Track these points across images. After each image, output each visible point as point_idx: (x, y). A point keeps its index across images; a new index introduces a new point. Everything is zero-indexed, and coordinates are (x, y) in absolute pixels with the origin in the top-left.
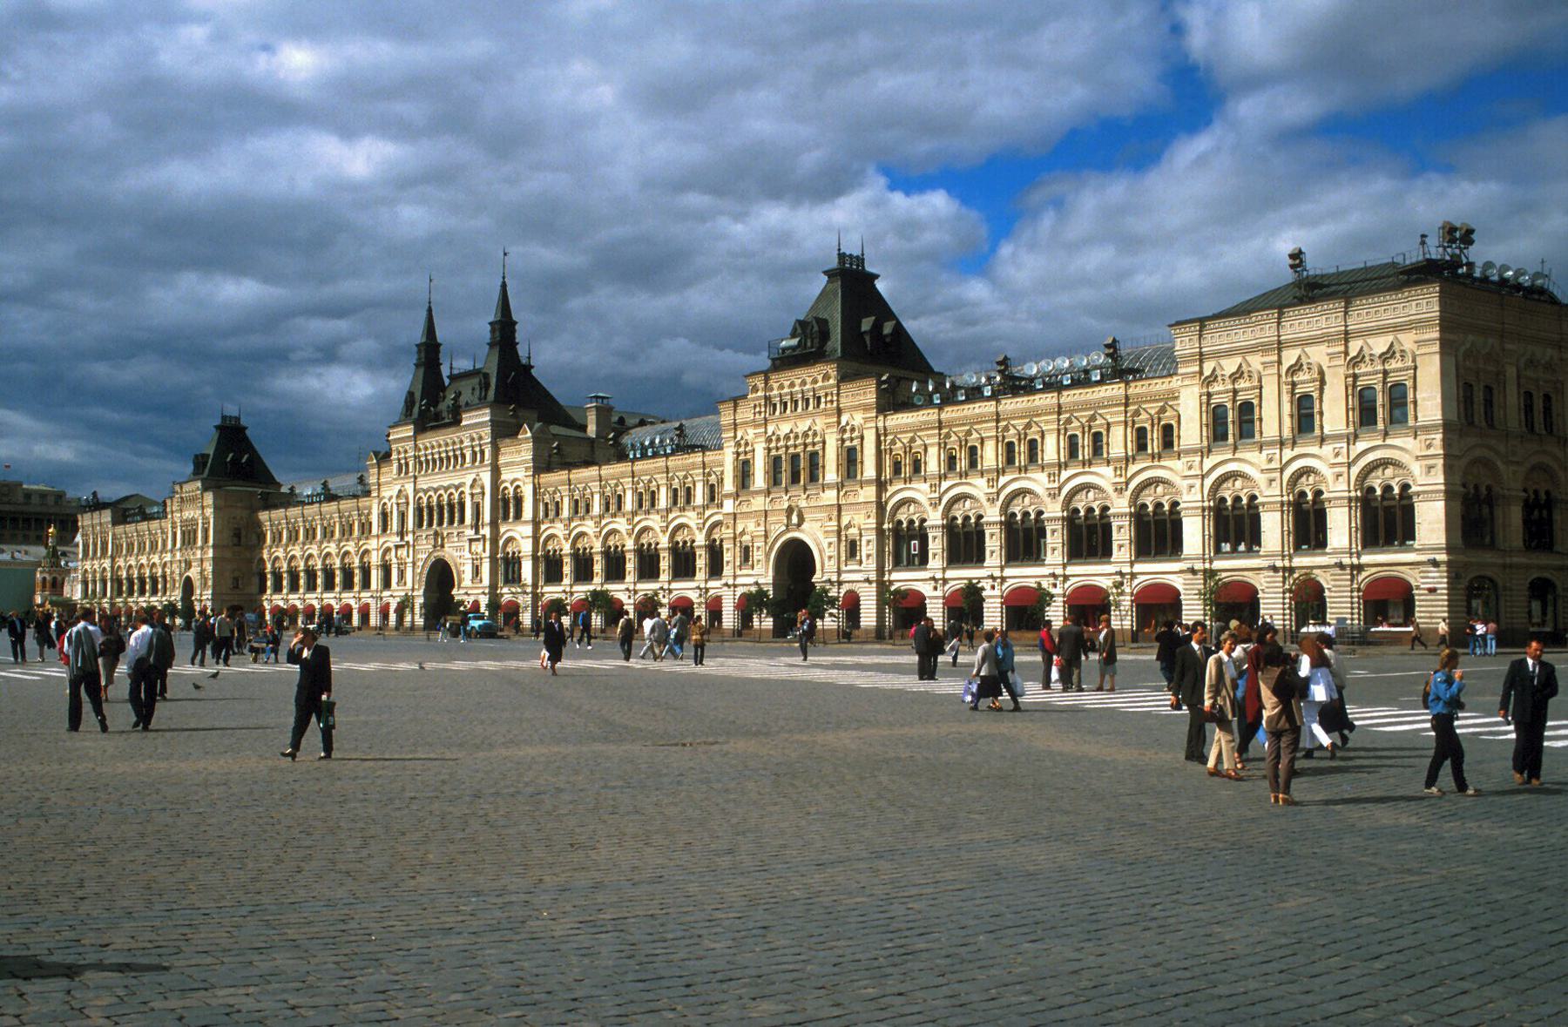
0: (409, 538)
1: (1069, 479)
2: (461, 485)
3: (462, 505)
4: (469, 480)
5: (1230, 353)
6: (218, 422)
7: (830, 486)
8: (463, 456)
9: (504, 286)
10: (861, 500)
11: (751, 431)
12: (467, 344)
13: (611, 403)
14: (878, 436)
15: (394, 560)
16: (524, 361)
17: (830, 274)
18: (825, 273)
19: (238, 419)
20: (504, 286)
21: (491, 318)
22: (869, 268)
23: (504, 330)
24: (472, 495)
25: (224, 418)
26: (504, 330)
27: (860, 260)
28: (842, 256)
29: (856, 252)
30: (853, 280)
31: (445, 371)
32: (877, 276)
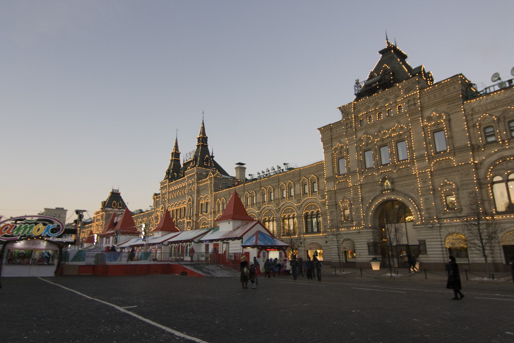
13: (245, 166)
18: (381, 52)
19: (118, 191)
23: (203, 140)
25: (113, 190)
26: (203, 140)
31: (182, 163)
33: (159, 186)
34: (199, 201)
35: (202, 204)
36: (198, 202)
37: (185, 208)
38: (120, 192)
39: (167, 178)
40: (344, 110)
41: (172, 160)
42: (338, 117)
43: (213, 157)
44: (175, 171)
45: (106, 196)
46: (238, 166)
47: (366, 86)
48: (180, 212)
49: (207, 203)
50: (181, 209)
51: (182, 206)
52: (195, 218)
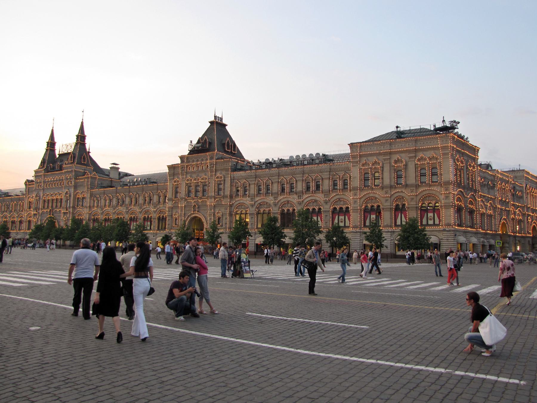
1: (305, 199)
5: (371, 155)
7: (211, 197)
9: (82, 123)
12: (65, 143)
14: (231, 180)
16: (88, 150)
17: (211, 123)
18: (210, 122)
20: (82, 123)
22: (224, 122)
23: (81, 138)
26: (81, 138)
28: (215, 117)
29: (220, 116)
30: (218, 126)
33: (33, 174)
34: (76, 195)
35: (78, 198)
36: (75, 196)
37: (61, 199)
39: (41, 168)
40: (182, 158)
41: (47, 150)
42: (178, 161)
43: (89, 152)
44: (52, 161)
46: (113, 165)
47: (194, 147)
48: (57, 202)
49: (83, 198)
50: (57, 199)
51: (59, 197)
52: (71, 210)
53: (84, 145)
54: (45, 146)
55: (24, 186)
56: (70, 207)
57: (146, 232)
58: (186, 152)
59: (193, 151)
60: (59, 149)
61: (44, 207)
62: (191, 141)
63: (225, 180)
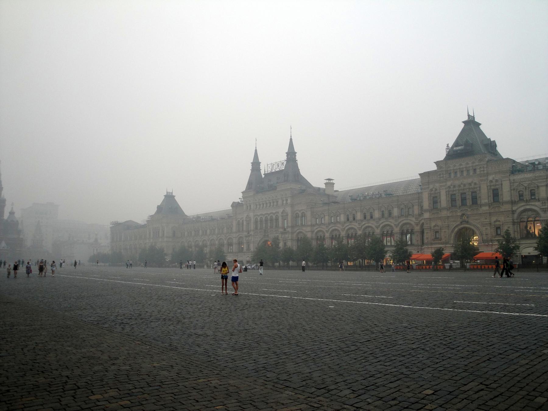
0: (252, 233)
2: (278, 212)
3: (277, 219)
4: (281, 210)
6: (165, 194)
7: (485, 205)
8: (277, 202)
10: (501, 210)
11: (437, 185)
13: (333, 181)
15: (245, 241)
18: (463, 122)
20: (291, 140)
21: (287, 151)
23: (291, 155)
24: (282, 216)
26: (291, 155)
27: (474, 117)
28: (469, 115)
31: (262, 172)
32: (480, 124)
33: (241, 195)
38: (174, 194)
40: (437, 163)
42: (434, 168)
45: (159, 200)
53: (295, 161)
54: (250, 167)
55: (231, 208)
56: (288, 227)
57: (407, 248)
58: (442, 156)
59: (453, 154)
60: (264, 169)
61: (256, 228)
62: (448, 145)
63: (502, 184)
